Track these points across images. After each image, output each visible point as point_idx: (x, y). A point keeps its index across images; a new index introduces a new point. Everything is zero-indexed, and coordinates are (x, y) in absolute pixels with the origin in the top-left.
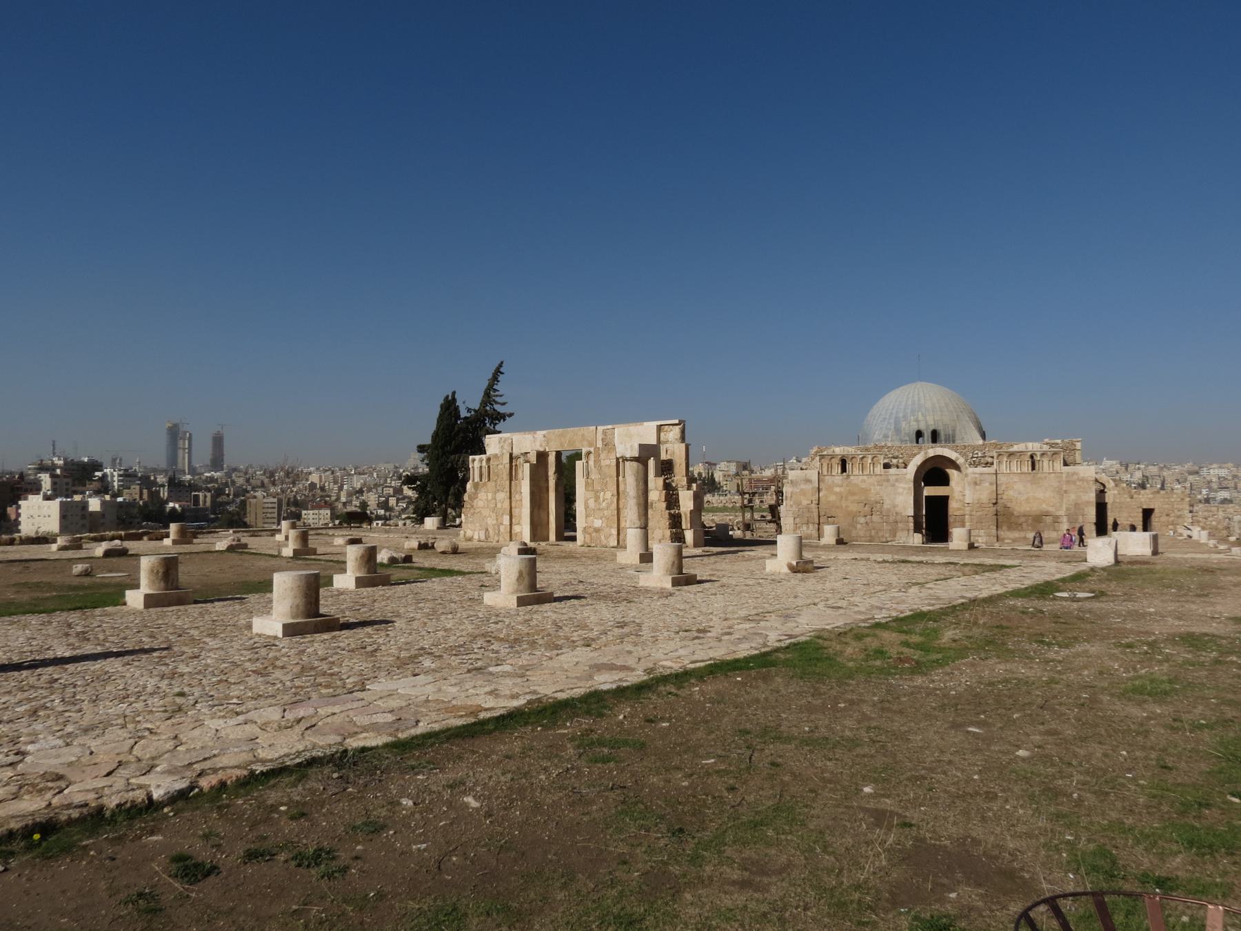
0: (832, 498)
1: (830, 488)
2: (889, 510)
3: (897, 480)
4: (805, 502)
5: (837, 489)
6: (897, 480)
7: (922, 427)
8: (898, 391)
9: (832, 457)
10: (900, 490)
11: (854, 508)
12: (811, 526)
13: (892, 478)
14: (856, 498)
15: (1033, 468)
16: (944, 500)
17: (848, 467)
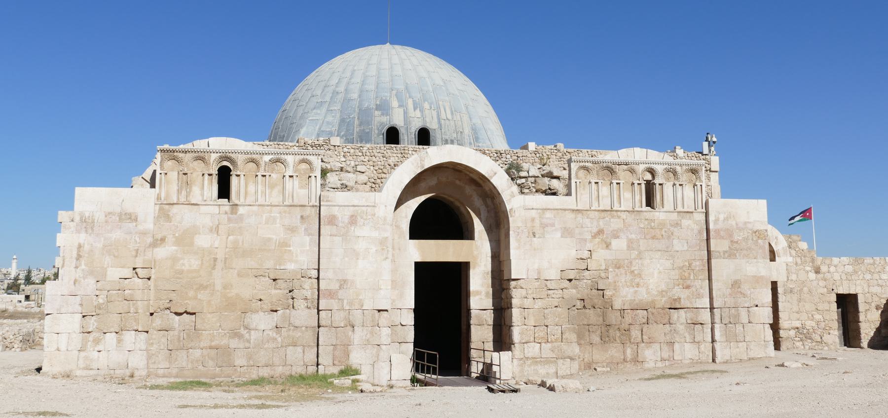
0: (190, 263)
1: (185, 239)
2: (331, 294)
3: (353, 220)
4: (114, 274)
5: (203, 241)
6: (353, 220)
7: (398, 121)
8: (349, 55)
9: (201, 157)
10: (361, 246)
11: (245, 289)
12: (129, 337)
13: (343, 215)
14: (251, 263)
15: (650, 202)
16: (457, 273)
17: (234, 183)
